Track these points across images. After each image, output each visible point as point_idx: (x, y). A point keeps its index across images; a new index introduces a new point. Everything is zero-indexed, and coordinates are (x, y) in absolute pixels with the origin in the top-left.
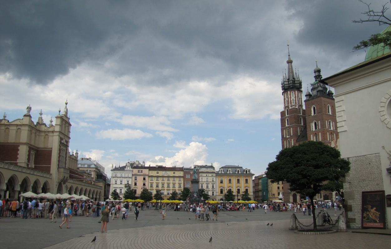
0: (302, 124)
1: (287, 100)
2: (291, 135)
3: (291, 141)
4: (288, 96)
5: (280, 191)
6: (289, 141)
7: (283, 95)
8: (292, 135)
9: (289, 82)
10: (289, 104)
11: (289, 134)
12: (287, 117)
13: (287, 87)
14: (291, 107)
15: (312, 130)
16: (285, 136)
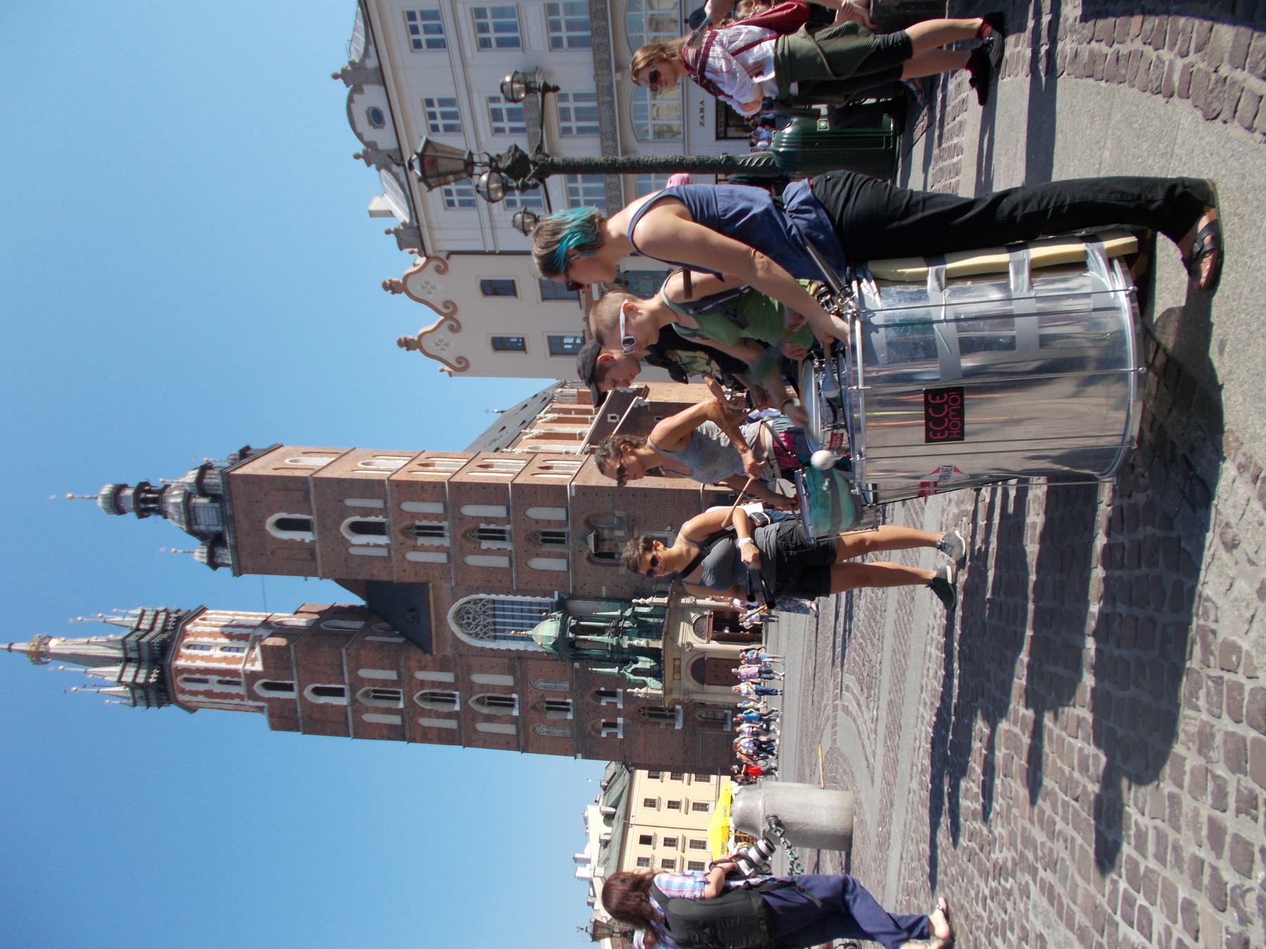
0: (358, 624)
1: (216, 678)
2: (393, 683)
3: (422, 684)
4: (198, 670)
5: (683, 860)
6: (424, 697)
7: (191, 709)
8: (391, 675)
9: (133, 655)
10: (235, 673)
11: (384, 693)
12: (301, 692)
13: (148, 677)
14: (255, 660)
15: (384, 553)
16: (396, 720)
